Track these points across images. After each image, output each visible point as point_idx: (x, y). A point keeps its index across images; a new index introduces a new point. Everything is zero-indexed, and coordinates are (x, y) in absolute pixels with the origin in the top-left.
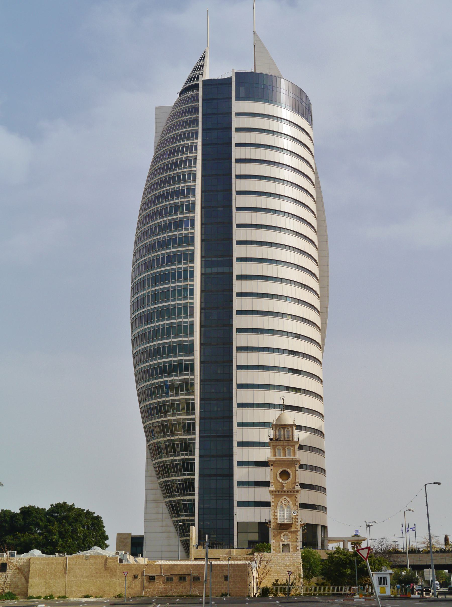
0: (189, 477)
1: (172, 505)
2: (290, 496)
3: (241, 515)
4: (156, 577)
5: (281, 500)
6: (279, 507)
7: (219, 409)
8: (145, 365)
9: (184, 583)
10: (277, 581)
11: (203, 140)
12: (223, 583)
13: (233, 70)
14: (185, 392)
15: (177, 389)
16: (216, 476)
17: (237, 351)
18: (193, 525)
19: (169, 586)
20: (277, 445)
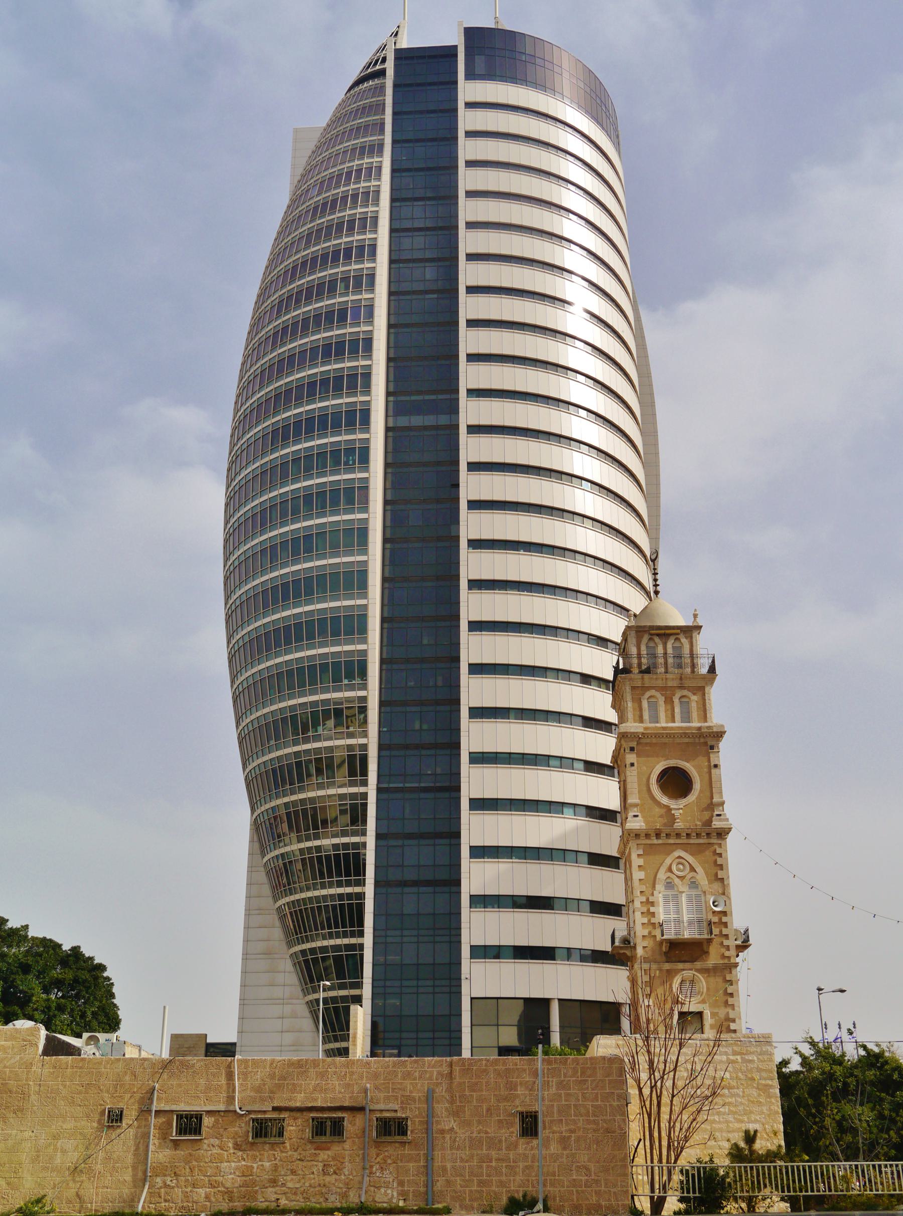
0: (349, 890)
1: (306, 962)
2: (696, 850)
3: (480, 980)
4: (207, 1121)
5: (668, 861)
6: (660, 887)
7: (425, 727)
8: (266, 711)
9: (336, 1149)
10: (750, 1138)
11: (393, 161)
12: (513, 1146)
13: (460, 23)
14: (346, 682)
15: (326, 714)
16: (416, 883)
17: (470, 588)
18: (358, 1000)
19: (263, 1162)
20: (645, 689)
